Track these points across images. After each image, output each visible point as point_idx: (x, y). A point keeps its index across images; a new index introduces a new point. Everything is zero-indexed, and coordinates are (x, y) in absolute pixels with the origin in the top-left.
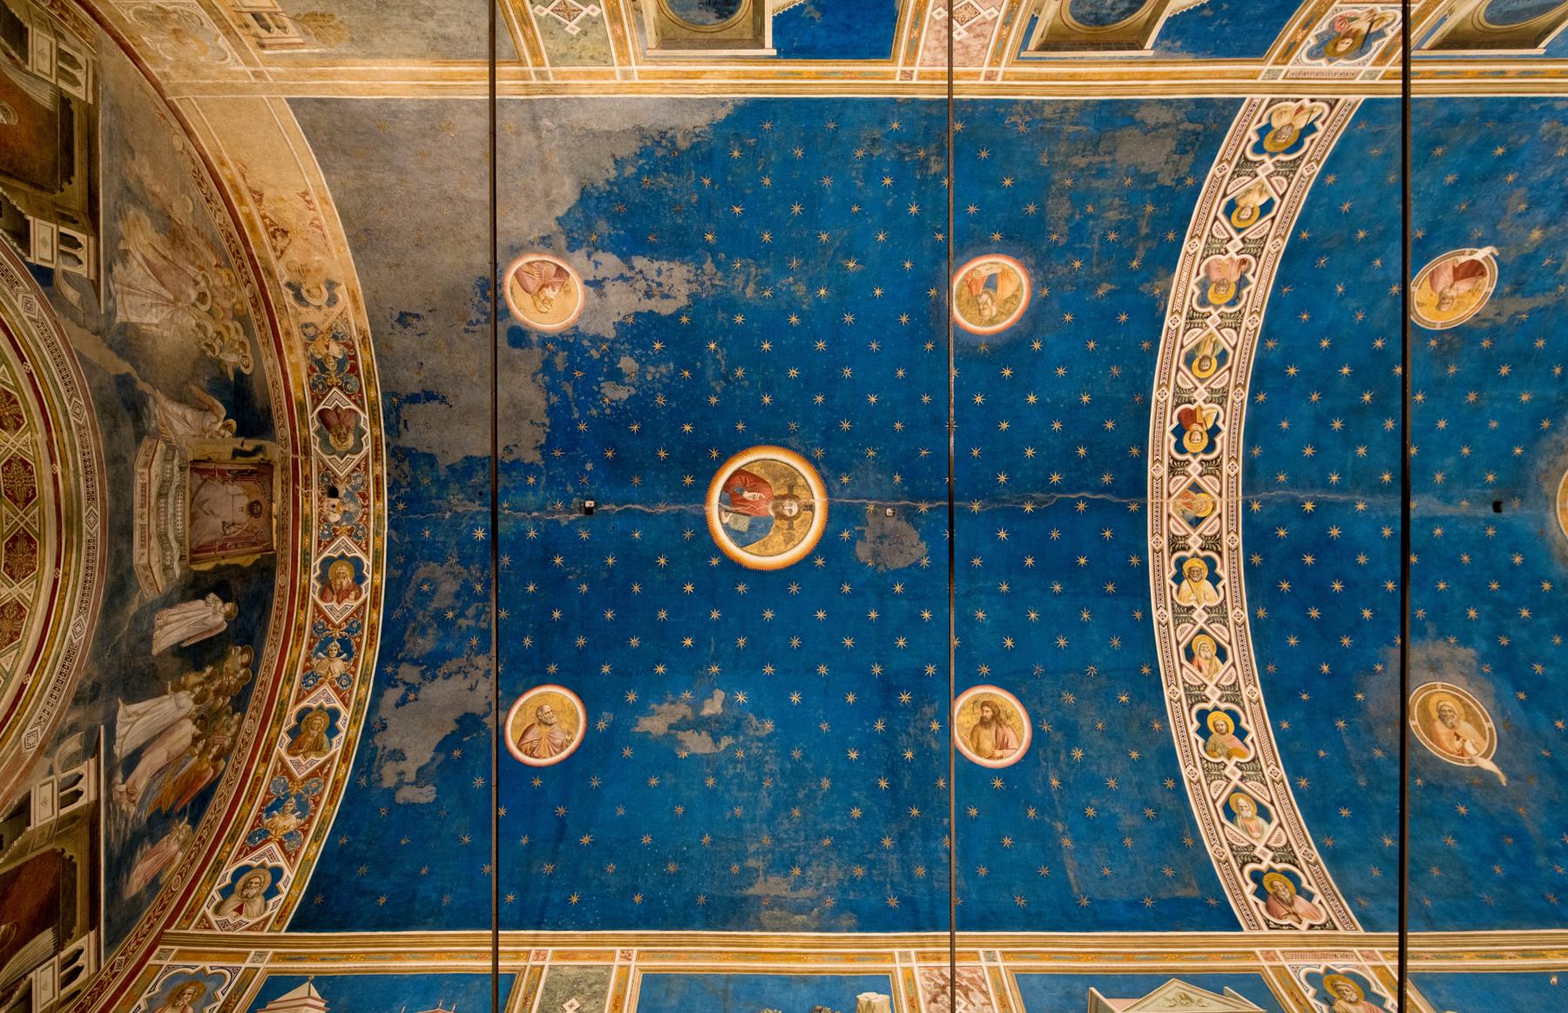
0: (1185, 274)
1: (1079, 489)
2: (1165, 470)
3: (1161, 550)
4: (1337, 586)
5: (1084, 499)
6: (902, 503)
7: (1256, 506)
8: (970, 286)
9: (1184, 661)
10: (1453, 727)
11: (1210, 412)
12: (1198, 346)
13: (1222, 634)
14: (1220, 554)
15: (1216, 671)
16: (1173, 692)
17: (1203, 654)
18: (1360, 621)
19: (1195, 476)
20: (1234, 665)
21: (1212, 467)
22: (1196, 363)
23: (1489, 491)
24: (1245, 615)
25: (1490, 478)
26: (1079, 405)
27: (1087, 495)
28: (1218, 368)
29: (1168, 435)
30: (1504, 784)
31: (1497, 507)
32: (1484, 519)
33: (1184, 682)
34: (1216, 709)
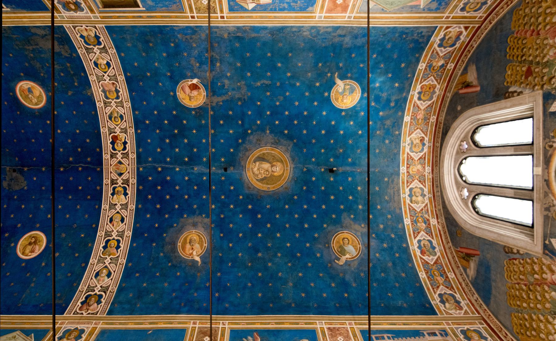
0: (95, 88)
1: (79, 163)
2: (109, 156)
3: (108, 184)
4: (168, 197)
5: (81, 166)
6: (19, 167)
7: (141, 169)
8: (23, 92)
9: (108, 223)
10: (193, 245)
11: (122, 136)
12: (111, 113)
13: (124, 213)
14: (128, 186)
15: (119, 226)
16: (101, 233)
17: (116, 220)
18: (174, 209)
19: (120, 158)
20: (125, 224)
21: (126, 155)
22: (113, 119)
23: (222, 164)
24: (134, 207)
25: (223, 160)
26: (76, 133)
27: (82, 165)
28: (121, 121)
29: (109, 144)
30: (199, 265)
31: (226, 170)
32: (221, 174)
33: (106, 230)
34: (114, 239)
